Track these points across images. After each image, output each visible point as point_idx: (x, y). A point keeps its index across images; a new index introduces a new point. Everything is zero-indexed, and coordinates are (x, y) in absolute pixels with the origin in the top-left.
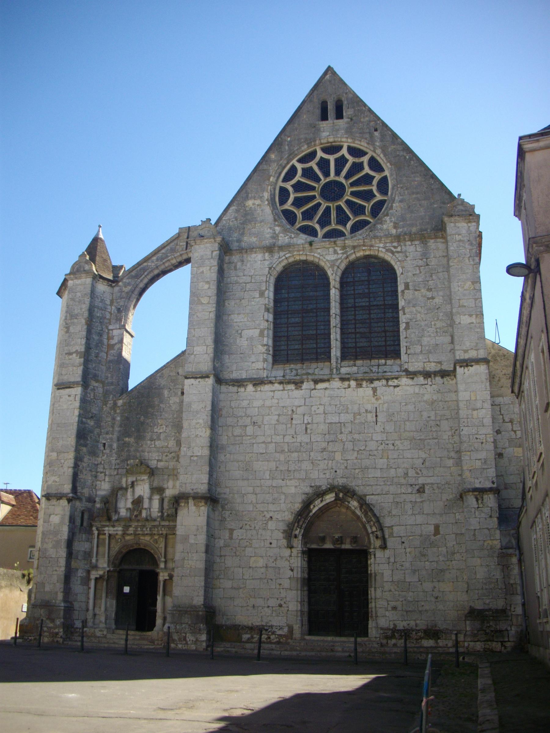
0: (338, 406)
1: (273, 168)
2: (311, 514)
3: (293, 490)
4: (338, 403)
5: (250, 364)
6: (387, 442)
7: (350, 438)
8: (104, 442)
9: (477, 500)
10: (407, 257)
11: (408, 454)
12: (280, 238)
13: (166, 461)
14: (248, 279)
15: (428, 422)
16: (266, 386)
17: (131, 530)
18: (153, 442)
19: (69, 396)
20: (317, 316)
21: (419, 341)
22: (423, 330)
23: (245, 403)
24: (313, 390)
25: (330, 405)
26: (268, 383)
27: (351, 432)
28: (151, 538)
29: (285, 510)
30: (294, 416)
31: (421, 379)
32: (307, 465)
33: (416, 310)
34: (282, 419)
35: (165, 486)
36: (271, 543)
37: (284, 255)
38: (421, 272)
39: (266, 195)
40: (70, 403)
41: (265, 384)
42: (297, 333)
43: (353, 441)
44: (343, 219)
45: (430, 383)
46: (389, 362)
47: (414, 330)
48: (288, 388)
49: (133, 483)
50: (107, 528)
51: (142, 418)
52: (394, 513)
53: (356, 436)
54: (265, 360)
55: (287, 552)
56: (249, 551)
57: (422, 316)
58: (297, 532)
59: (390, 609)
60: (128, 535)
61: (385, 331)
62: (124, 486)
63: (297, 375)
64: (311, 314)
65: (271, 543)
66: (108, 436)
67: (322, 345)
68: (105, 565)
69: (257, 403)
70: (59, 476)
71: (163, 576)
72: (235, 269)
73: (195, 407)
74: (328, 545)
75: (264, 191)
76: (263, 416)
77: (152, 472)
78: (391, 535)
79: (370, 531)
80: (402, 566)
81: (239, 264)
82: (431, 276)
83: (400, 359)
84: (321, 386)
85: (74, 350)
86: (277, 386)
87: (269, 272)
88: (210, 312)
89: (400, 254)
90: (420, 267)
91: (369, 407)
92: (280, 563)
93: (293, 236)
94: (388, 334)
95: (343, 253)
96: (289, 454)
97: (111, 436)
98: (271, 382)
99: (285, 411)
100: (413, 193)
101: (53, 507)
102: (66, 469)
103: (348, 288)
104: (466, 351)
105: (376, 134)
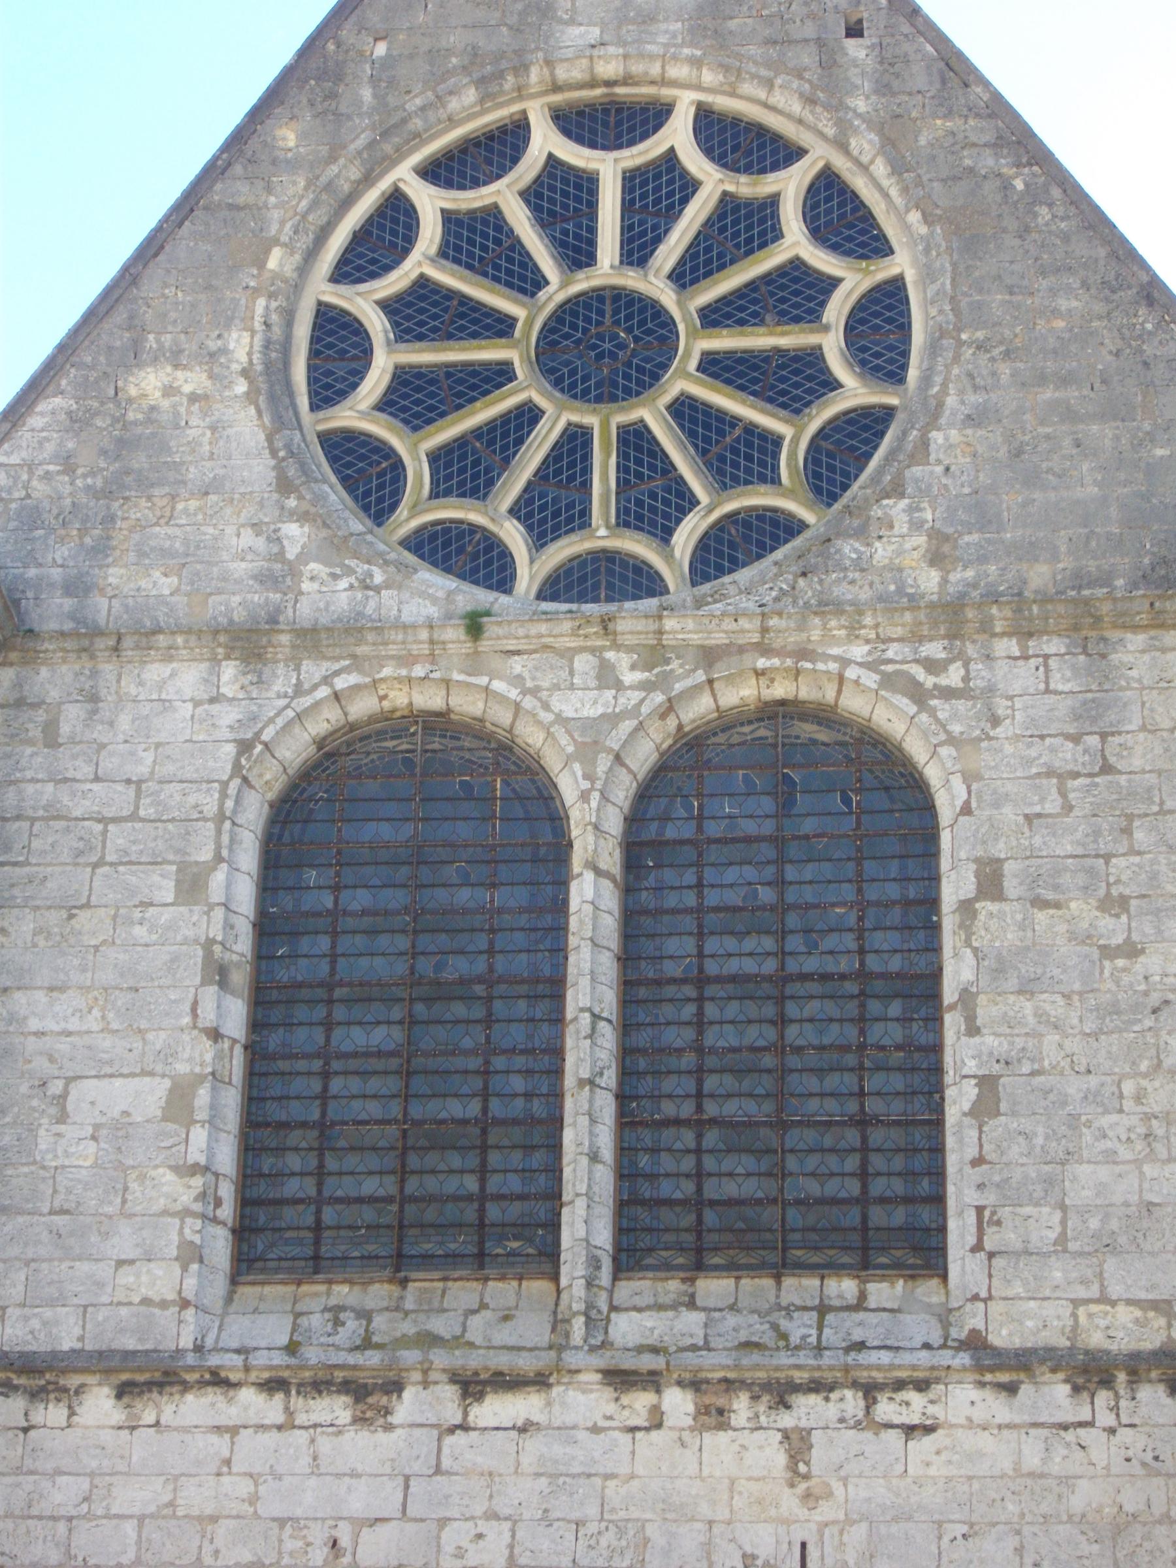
0: (593, 1527)
1: (286, 201)
4: (593, 1511)
10: (996, 721)
12: (306, 586)
14: (120, 799)
16: (190, 1397)
20: (489, 1021)
21: (1049, 1182)
22: (1073, 1121)
23: (64, 1494)
24: (452, 1430)
25: (547, 1519)
26: (202, 1384)
31: (1055, 1396)
33: (1039, 1015)
37: (326, 680)
38: (1068, 808)
39: (241, 346)
41: (186, 1387)
42: (374, 1109)
44: (653, 500)
45: (1106, 1419)
46: (882, 1292)
47: (1025, 1124)
48: (315, 1418)
54: (191, 1254)
57: (1073, 1045)
61: (863, 1122)
63: (366, 1344)
64: (459, 1009)
67: (514, 1184)
72: (51, 738)
75: (228, 326)
81: (72, 717)
82: (1127, 831)
83: (944, 1277)
84: (496, 1409)
86: (251, 1403)
87: (237, 767)
89: (961, 705)
90: (1063, 777)
93: (378, 578)
94: (877, 1136)
95: (648, 687)
98: (218, 1381)
99: (290, 1545)
100: (1042, 379)
103: (669, 876)
105: (856, 49)
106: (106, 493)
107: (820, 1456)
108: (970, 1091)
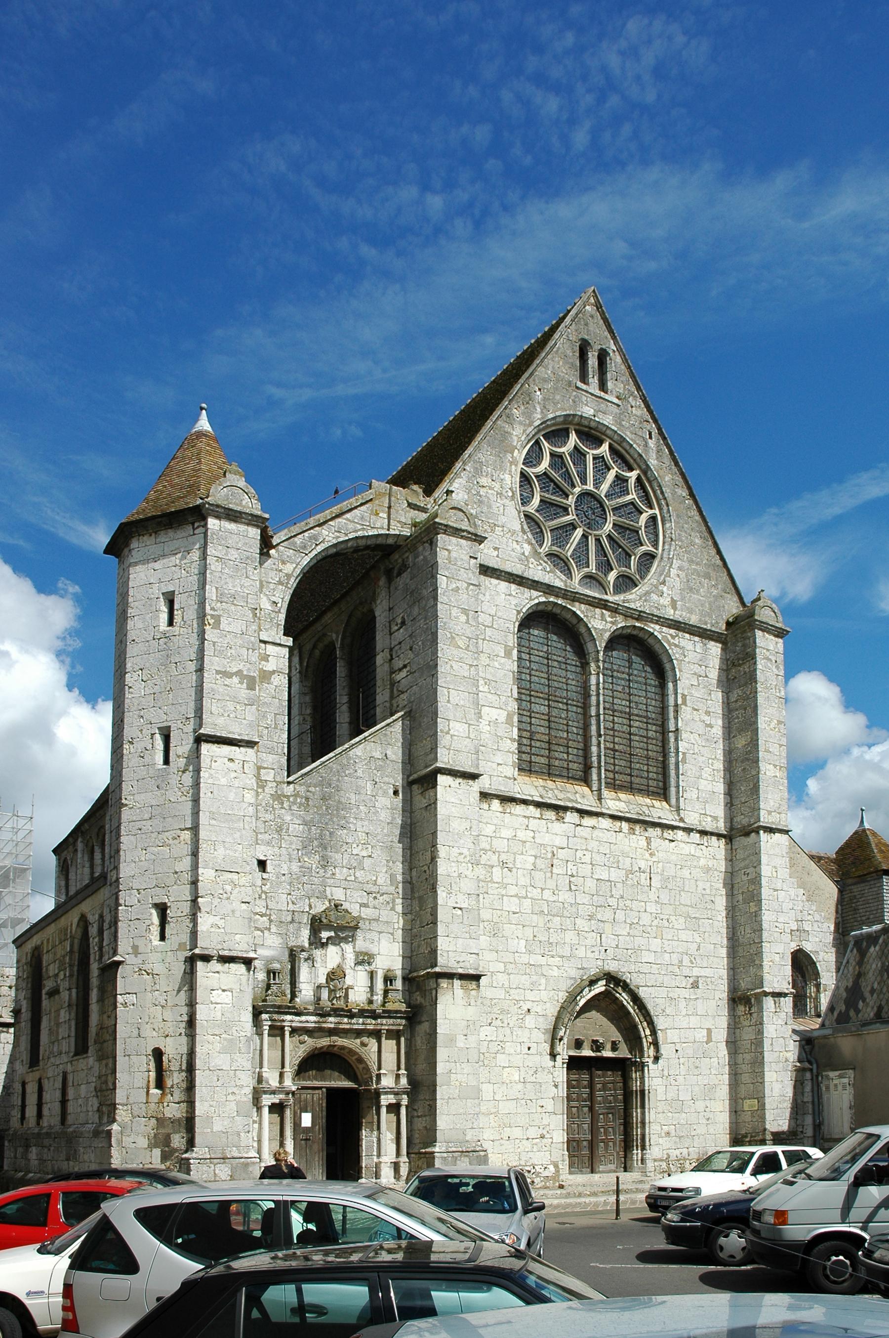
4: (608, 852)
5: (495, 766)
6: (662, 916)
11: (683, 936)
13: (375, 908)
15: (703, 895)
30: (555, 861)
34: (541, 864)
35: (374, 950)
37: (537, 597)
40: (233, 775)
52: (668, 1012)
53: (628, 903)
69: (506, 833)
84: (588, 821)
85: (235, 670)
91: (643, 865)
96: (550, 917)
98: (525, 802)
99: (543, 851)
101: (216, 975)
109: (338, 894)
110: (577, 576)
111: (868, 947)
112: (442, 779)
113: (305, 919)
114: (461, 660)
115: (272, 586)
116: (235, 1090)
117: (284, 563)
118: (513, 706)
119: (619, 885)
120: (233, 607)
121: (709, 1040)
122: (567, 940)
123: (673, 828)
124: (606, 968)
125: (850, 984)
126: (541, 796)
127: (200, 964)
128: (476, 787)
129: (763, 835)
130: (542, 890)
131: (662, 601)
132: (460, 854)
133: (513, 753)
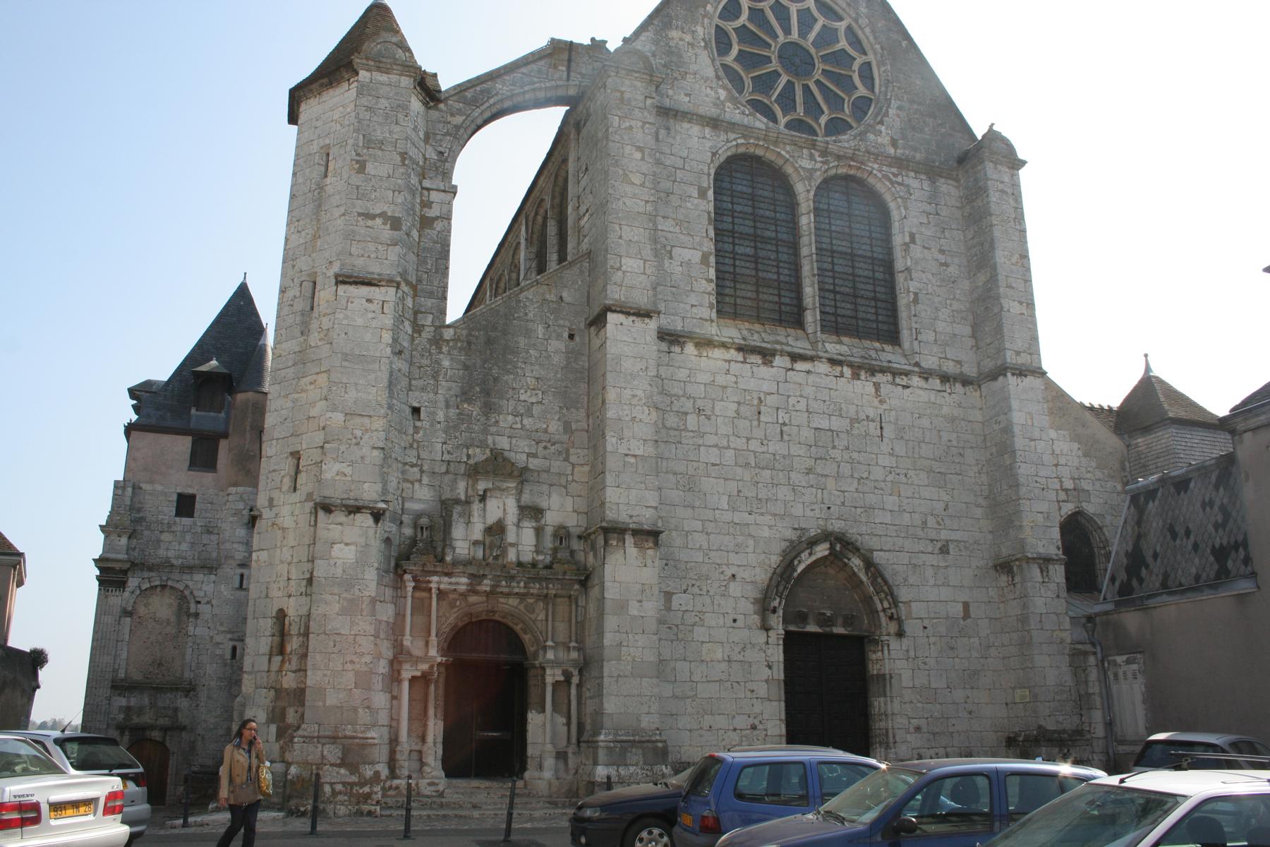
2: (796, 574)
3: (766, 533)
5: (688, 307)
7: (846, 457)
8: (416, 405)
9: (1042, 572)
14: (679, 163)
17: (486, 585)
18: (518, 419)
19: (369, 301)
23: (682, 374)
25: (815, 399)
27: (847, 448)
28: (520, 603)
29: (756, 566)
30: (763, 409)
32: (783, 493)
35: (544, 505)
36: (735, 621)
40: (370, 315)
41: (715, 347)
43: (851, 462)
46: (888, 348)
49: (485, 491)
50: (435, 578)
51: (495, 371)
52: (911, 581)
53: (855, 455)
55: (761, 637)
56: (700, 633)
58: (776, 603)
59: (912, 730)
60: (476, 592)
62: (463, 498)
64: (769, 247)
65: (735, 621)
66: (425, 396)
67: (788, 301)
68: (433, 652)
69: (703, 378)
70: (352, 464)
71: (554, 675)
73: (627, 365)
74: (812, 628)
76: (713, 400)
77: (522, 475)
78: (909, 616)
79: (879, 607)
80: (925, 663)
84: (800, 366)
88: (647, 202)
91: (871, 413)
92: (750, 655)
96: (757, 470)
97: (431, 395)
102: (366, 450)
104: (1018, 353)
106: (665, 66)
107: (883, 390)
108: (912, 296)
109: (503, 443)
110: (783, 121)
111: (1147, 503)
112: (611, 317)
113: (462, 468)
114: (635, 196)
115: (439, 137)
116: (354, 658)
117: (452, 115)
118: (710, 246)
119: (843, 436)
120: (380, 153)
121: (967, 615)
122: (780, 496)
123: (907, 374)
124: (830, 528)
125: (1130, 548)
126: (744, 339)
127: (321, 514)
128: (652, 325)
129: (1012, 380)
130: (748, 439)
131: (880, 140)
132: (634, 396)
133: (710, 294)
